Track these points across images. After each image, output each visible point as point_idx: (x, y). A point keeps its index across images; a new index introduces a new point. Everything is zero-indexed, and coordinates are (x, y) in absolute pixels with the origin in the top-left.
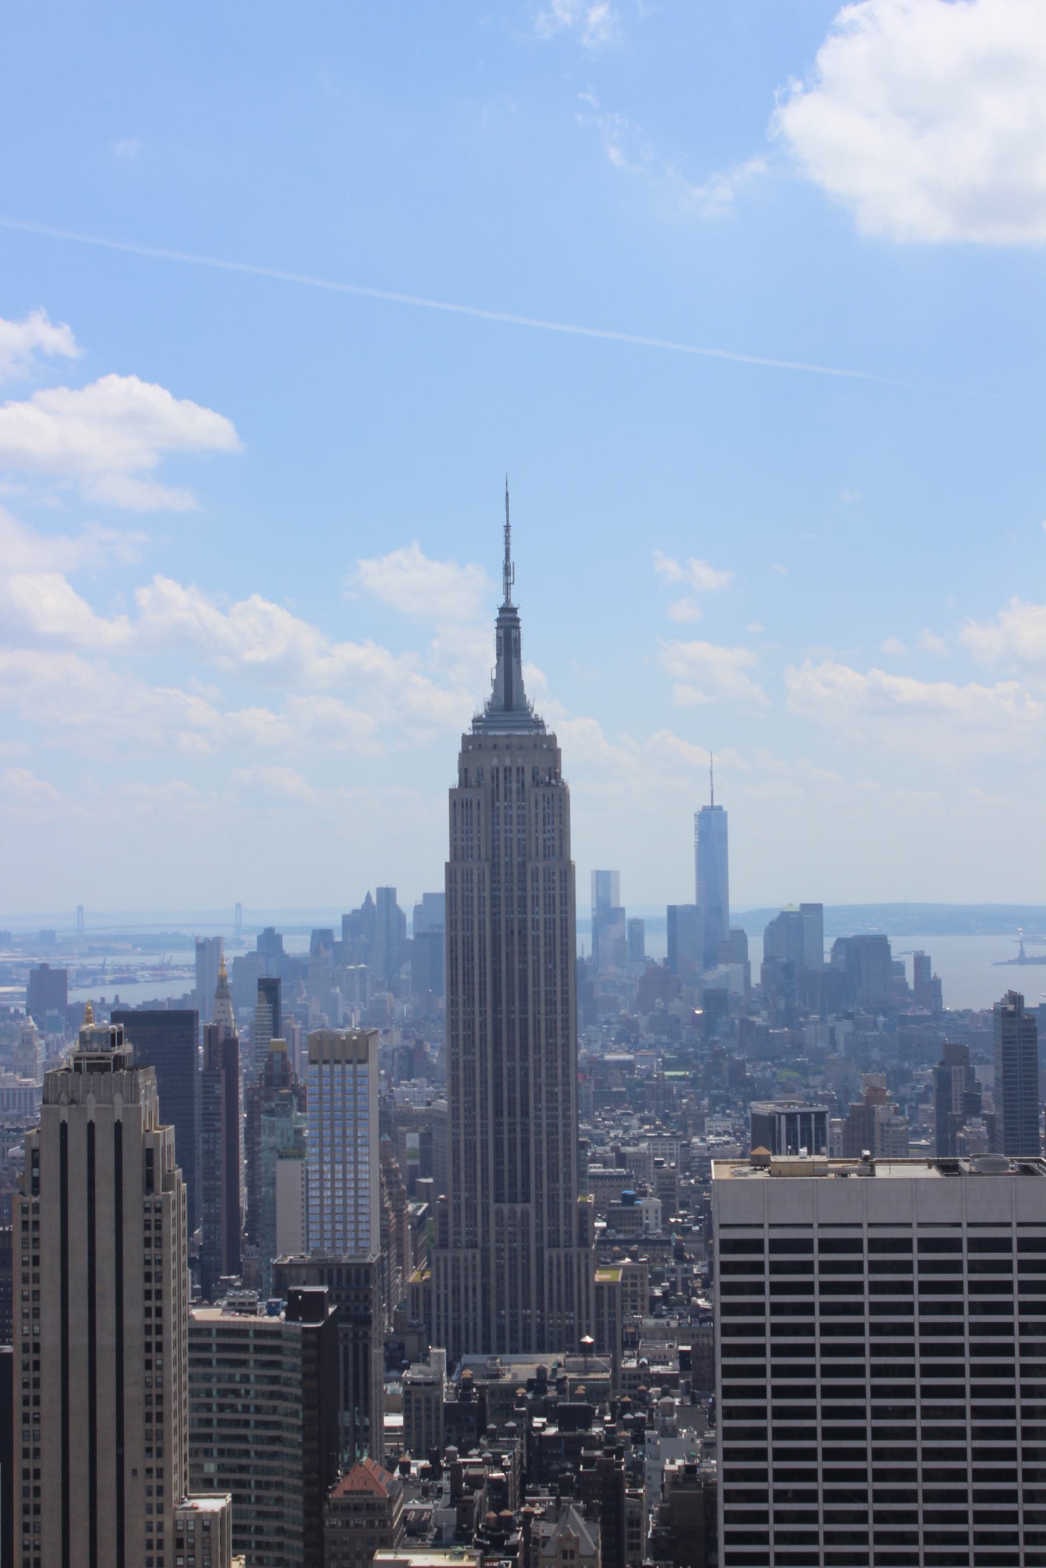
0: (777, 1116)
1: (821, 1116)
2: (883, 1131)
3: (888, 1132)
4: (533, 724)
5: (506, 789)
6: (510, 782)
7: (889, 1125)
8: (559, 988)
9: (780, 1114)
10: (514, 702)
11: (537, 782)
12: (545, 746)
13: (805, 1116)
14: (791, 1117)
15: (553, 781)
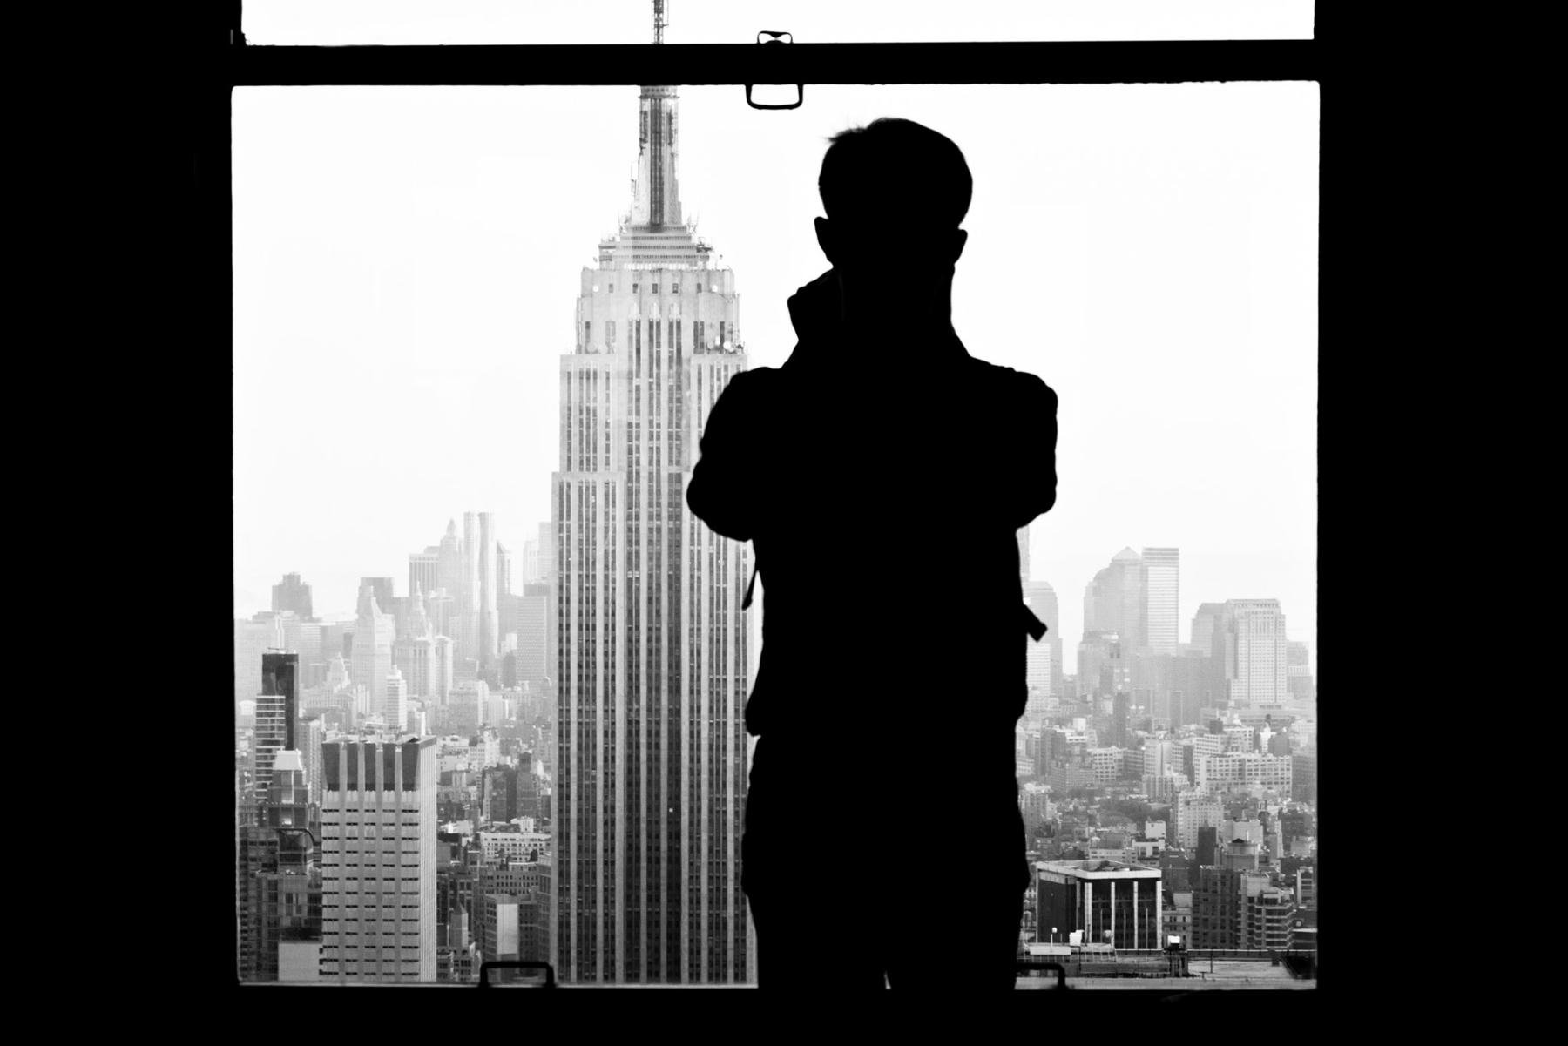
0: (1078, 883)
1: (1148, 885)
2: (1251, 909)
3: (1259, 912)
4: (694, 252)
5: (651, 356)
6: (659, 345)
7: (1262, 901)
8: (731, 677)
9: (1083, 881)
10: (666, 218)
11: (700, 346)
12: (715, 288)
13: (1124, 885)
14: (1101, 887)
15: (727, 345)
